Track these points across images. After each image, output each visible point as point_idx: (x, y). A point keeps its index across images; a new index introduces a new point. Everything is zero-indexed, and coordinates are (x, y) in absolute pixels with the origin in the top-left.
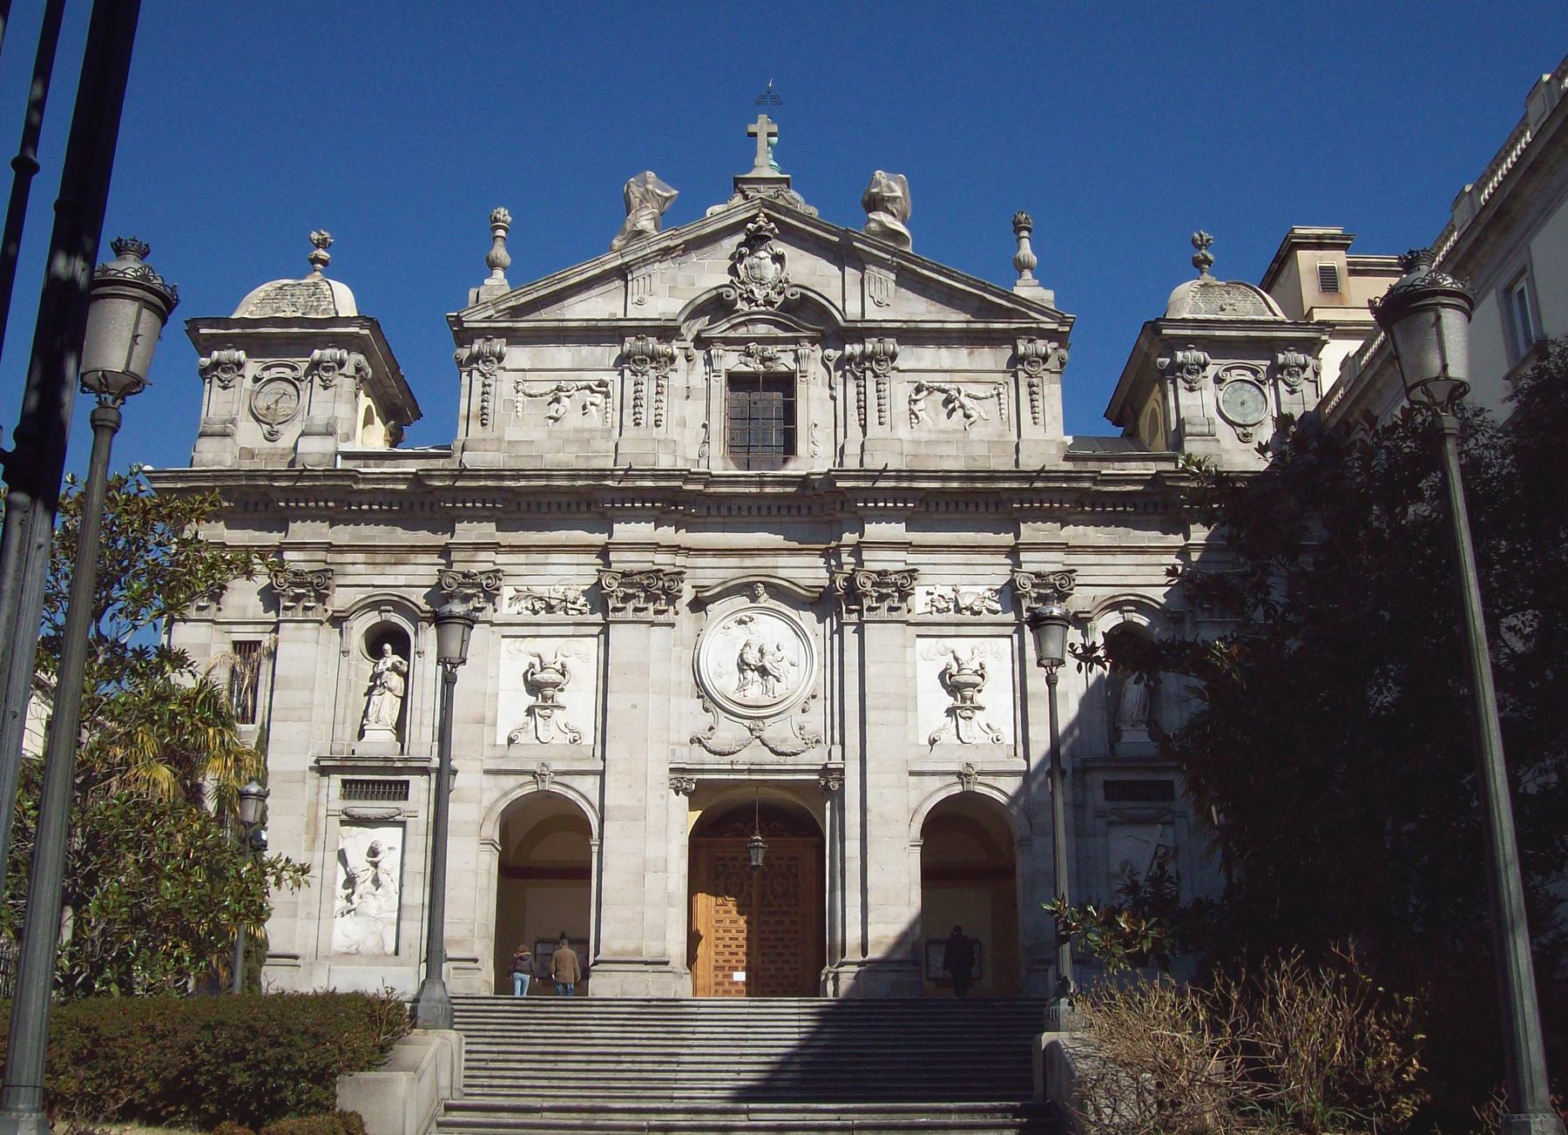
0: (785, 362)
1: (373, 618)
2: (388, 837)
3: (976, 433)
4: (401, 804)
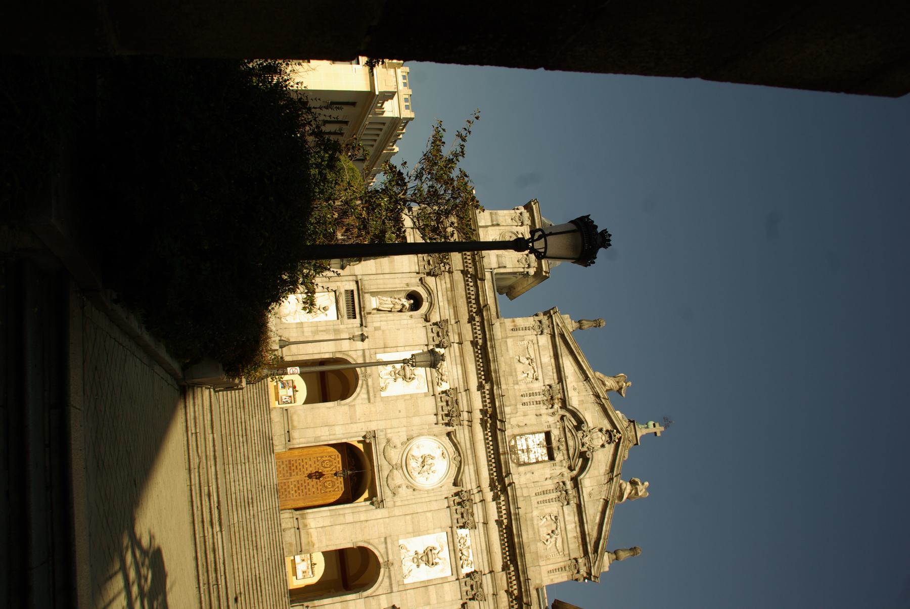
0: (558, 456)
1: (424, 294)
2: (332, 313)
3: (540, 545)
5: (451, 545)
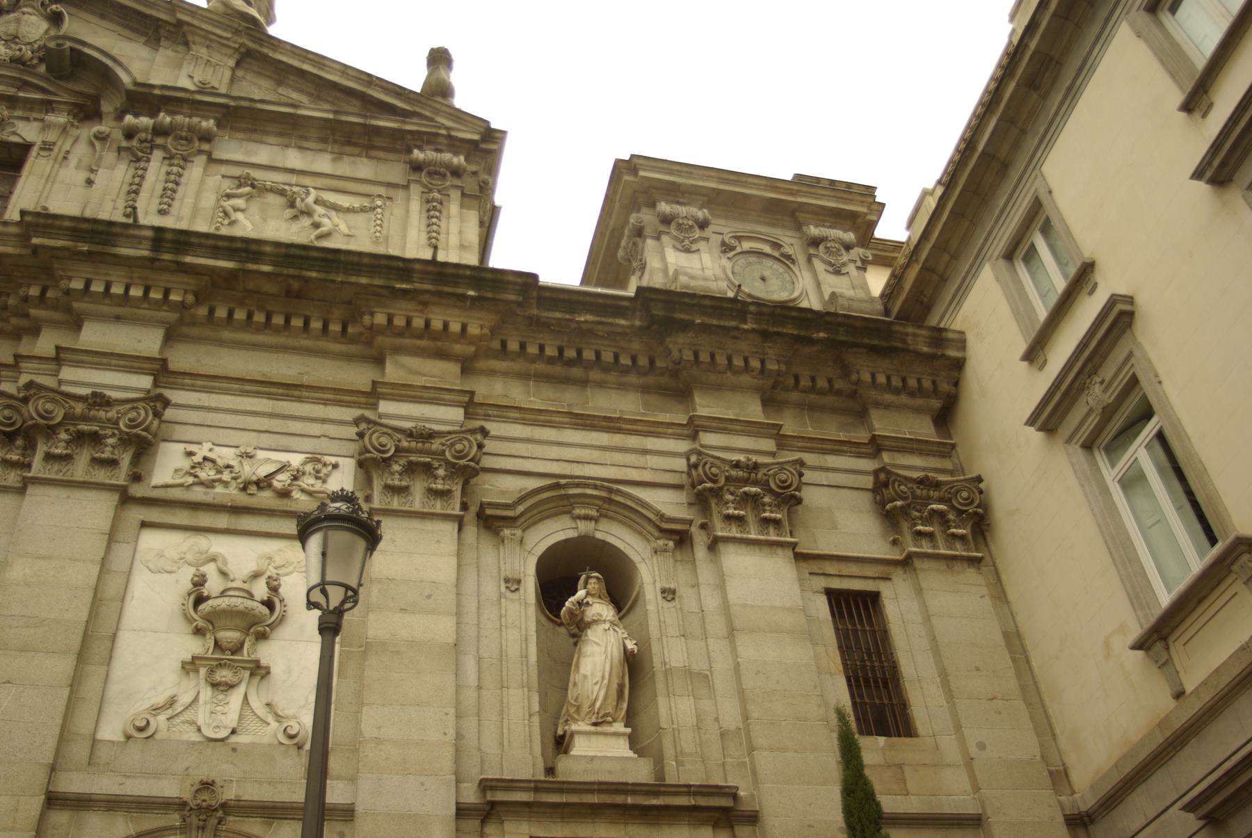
5: (205, 519)
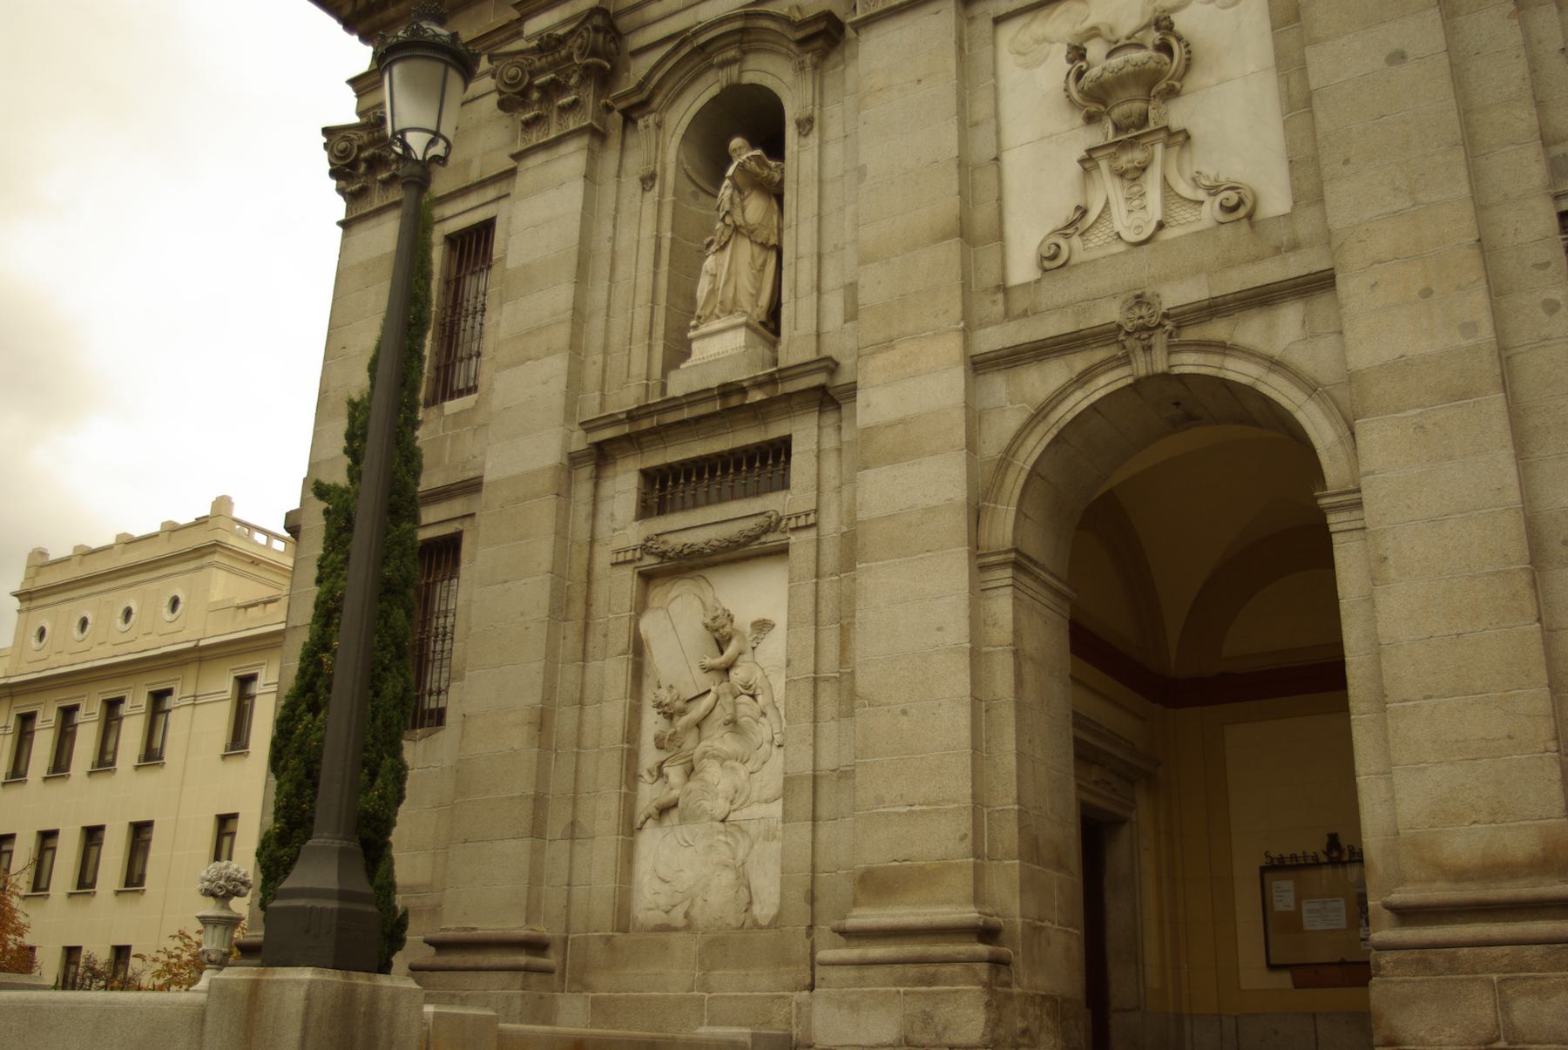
4: (774, 503)
